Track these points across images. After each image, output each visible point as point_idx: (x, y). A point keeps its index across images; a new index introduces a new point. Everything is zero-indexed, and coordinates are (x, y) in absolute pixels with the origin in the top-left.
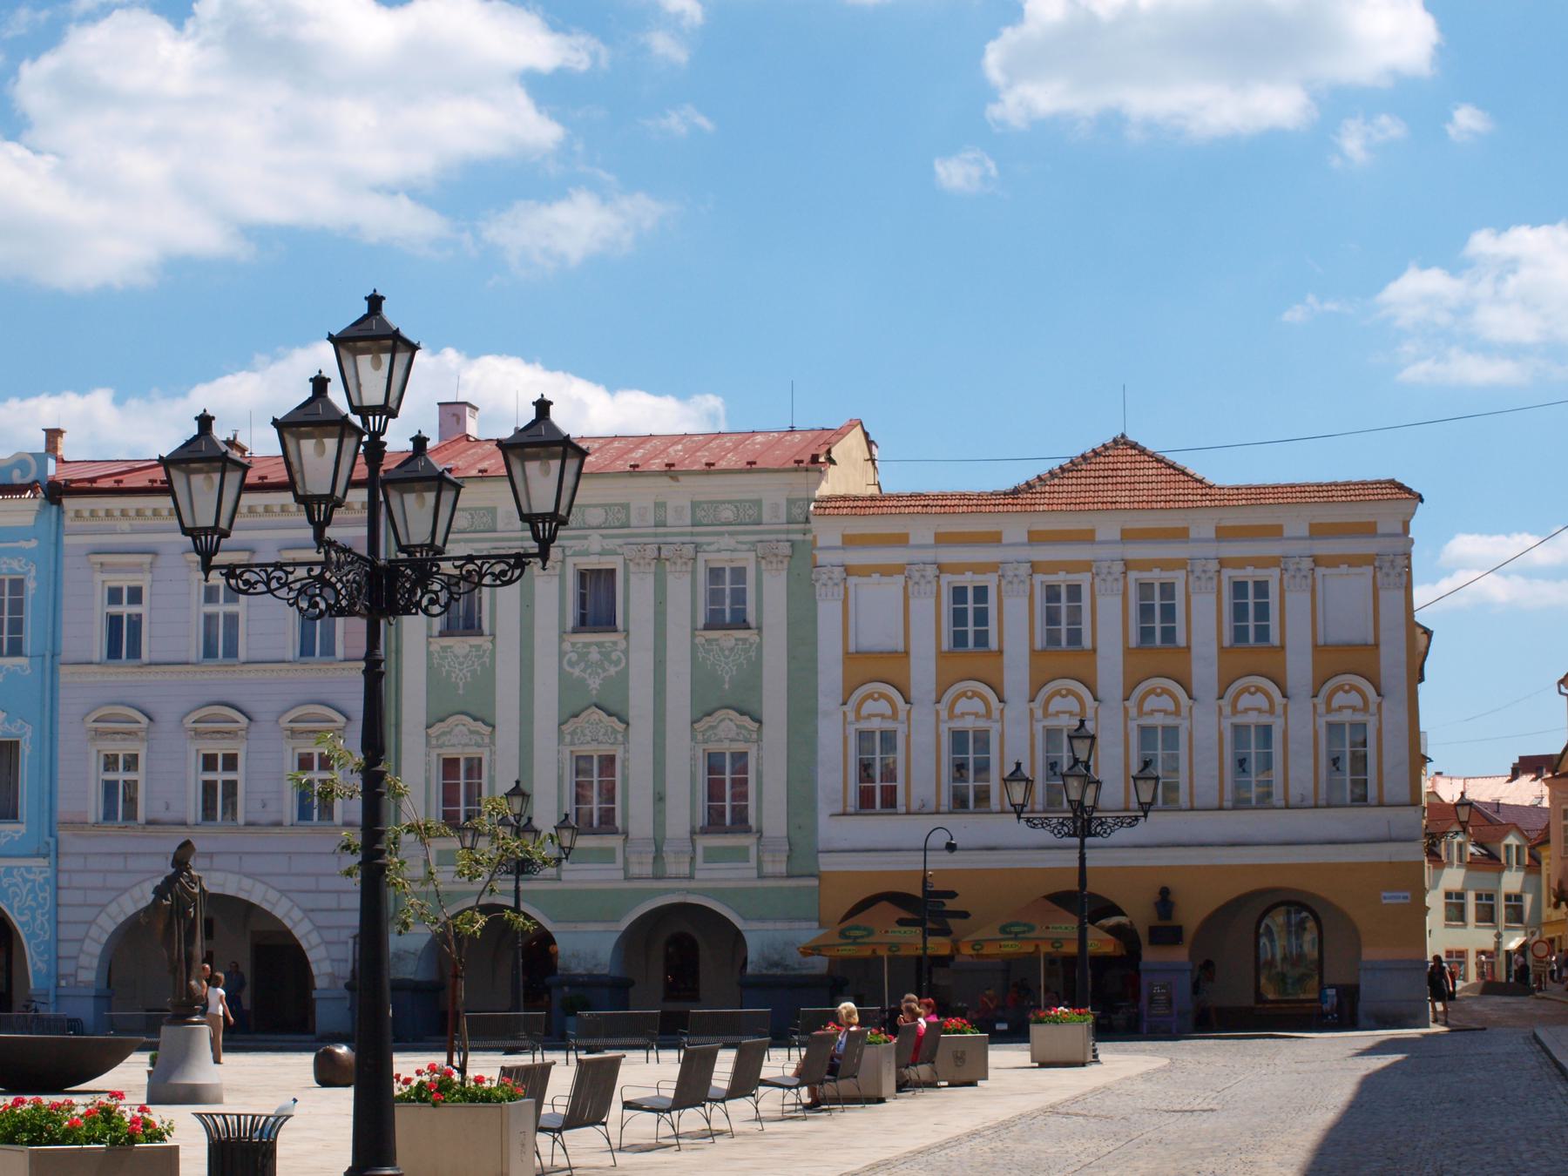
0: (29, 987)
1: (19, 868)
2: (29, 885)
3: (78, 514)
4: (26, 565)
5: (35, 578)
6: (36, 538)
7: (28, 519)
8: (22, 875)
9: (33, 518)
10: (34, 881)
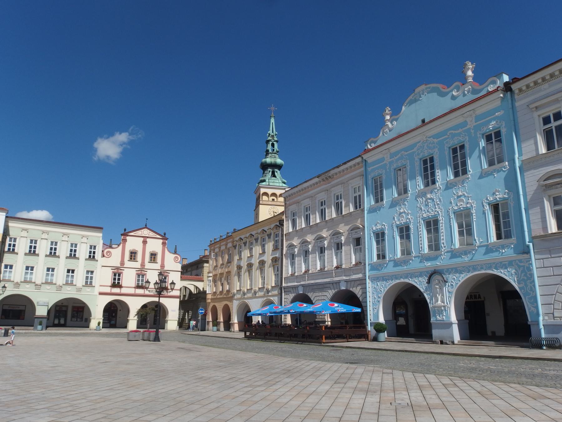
0: (528, 321)
1: (515, 260)
2: (521, 269)
3: (520, 90)
4: (500, 122)
5: (505, 127)
6: (503, 110)
7: (498, 103)
8: (517, 264)
9: (500, 102)
10: (524, 266)
